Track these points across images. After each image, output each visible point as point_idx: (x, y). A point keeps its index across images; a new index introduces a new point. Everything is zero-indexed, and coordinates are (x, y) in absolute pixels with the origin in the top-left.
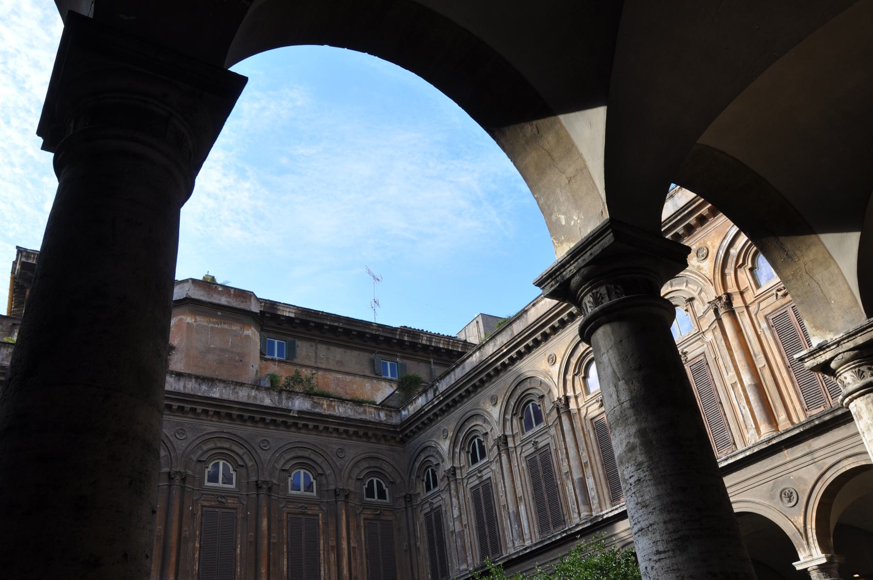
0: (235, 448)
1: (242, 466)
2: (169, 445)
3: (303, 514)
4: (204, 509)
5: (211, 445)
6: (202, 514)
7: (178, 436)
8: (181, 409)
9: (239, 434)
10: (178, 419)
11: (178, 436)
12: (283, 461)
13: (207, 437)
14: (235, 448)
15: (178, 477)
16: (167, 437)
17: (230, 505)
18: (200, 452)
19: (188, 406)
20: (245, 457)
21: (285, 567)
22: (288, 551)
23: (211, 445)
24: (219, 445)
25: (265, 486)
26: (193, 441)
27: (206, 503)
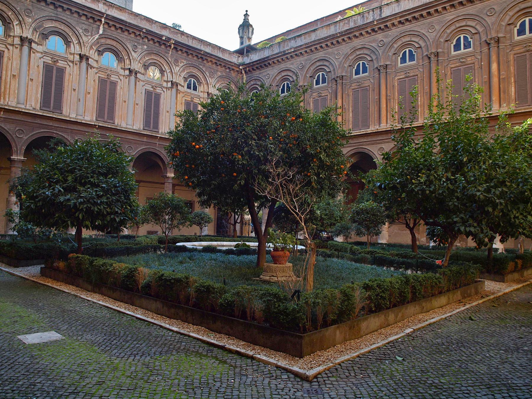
0: (469, 23)
1: (476, 33)
2: (425, 39)
3: (528, 51)
4: (452, 69)
5: (453, 28)
6: (451, 73)
7: (430, 31)
8: (429, 14)
9: (471, 13)
10: (430, 20)
11: (430, 31)
12: (508, 18)
13: (448, 24)
14: (469, 23)
15: (433, 56)
16: (424, 34)
17: (469, 62)
18: (446, 35)
19: (432, 10)
20: (477, 27)
21: (513, 94)
22: (515, 82)
23: (453, 28)
24: (458, 25)
25: (492, 42)
26: (440, 30)
27: (453, 66)
